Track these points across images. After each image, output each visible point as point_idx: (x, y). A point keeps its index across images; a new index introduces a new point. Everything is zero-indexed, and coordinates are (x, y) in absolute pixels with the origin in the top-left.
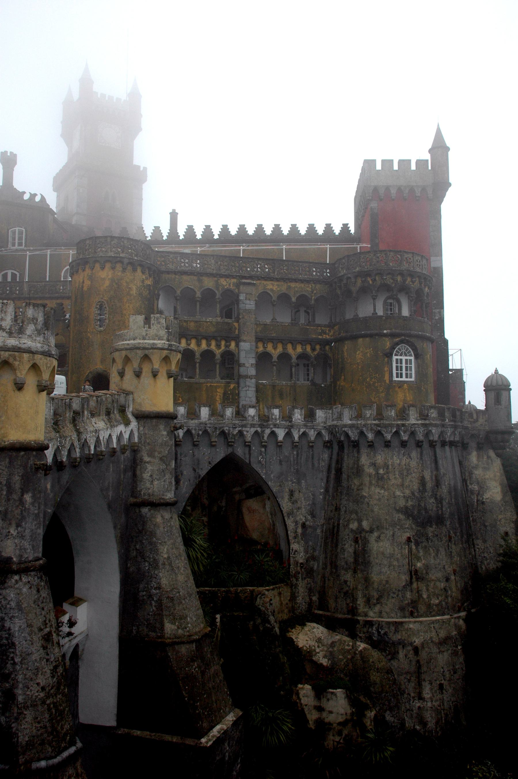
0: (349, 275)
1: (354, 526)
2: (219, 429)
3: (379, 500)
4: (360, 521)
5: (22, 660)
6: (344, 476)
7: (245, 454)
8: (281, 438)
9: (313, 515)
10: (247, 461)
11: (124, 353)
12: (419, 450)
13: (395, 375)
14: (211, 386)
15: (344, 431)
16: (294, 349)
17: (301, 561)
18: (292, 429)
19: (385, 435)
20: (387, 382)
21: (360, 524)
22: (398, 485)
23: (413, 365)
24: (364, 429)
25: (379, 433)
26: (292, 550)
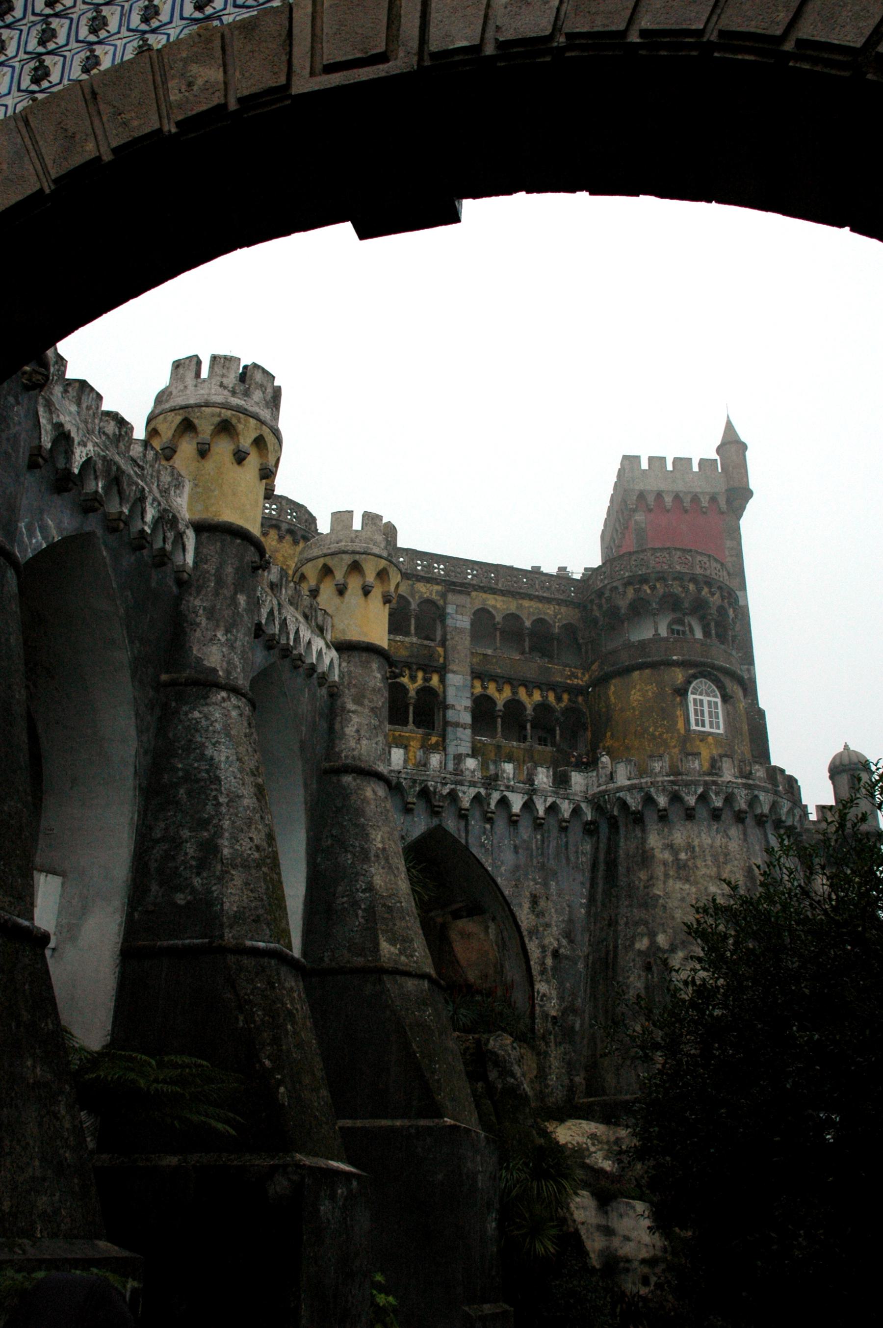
0: (614, 584)
1: (643, 944)
2: (420, 784)
3: (683, 899)
4: (652, 935)
5: (229, 801)
6: (622, 870)
7: (459, 830)
8: (516, 807)
9: (571, 941)
10: (463, 841)
11: (321, 561)
12: (740, 826)
13: (693, 721)
14: (400, 735)
15: (619, 798)
16: (530, 695)
17: (553, 1013)
18: (534, 797)
19: (687, 798)
20: (682, 731)
21: (653, 942)
22: (711, 877)
23: (720, 711)
24: (652, 790)
25: (675, 798)
26: (538, 992)
